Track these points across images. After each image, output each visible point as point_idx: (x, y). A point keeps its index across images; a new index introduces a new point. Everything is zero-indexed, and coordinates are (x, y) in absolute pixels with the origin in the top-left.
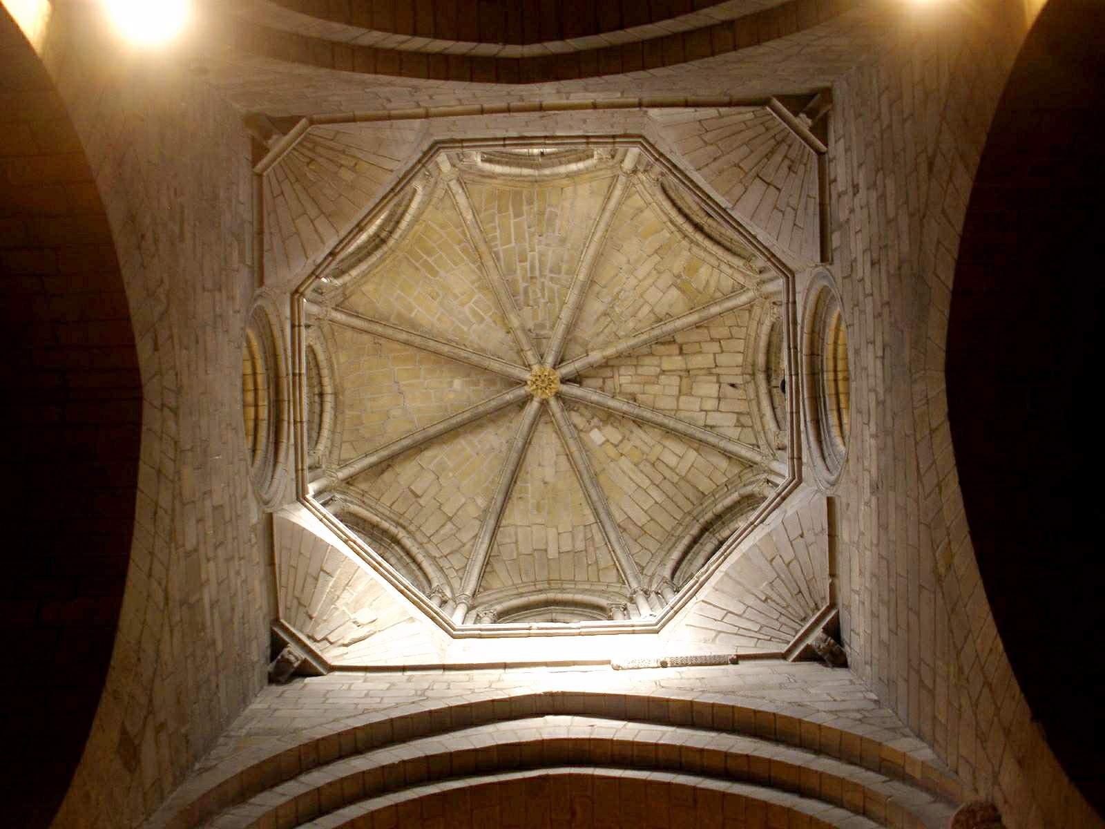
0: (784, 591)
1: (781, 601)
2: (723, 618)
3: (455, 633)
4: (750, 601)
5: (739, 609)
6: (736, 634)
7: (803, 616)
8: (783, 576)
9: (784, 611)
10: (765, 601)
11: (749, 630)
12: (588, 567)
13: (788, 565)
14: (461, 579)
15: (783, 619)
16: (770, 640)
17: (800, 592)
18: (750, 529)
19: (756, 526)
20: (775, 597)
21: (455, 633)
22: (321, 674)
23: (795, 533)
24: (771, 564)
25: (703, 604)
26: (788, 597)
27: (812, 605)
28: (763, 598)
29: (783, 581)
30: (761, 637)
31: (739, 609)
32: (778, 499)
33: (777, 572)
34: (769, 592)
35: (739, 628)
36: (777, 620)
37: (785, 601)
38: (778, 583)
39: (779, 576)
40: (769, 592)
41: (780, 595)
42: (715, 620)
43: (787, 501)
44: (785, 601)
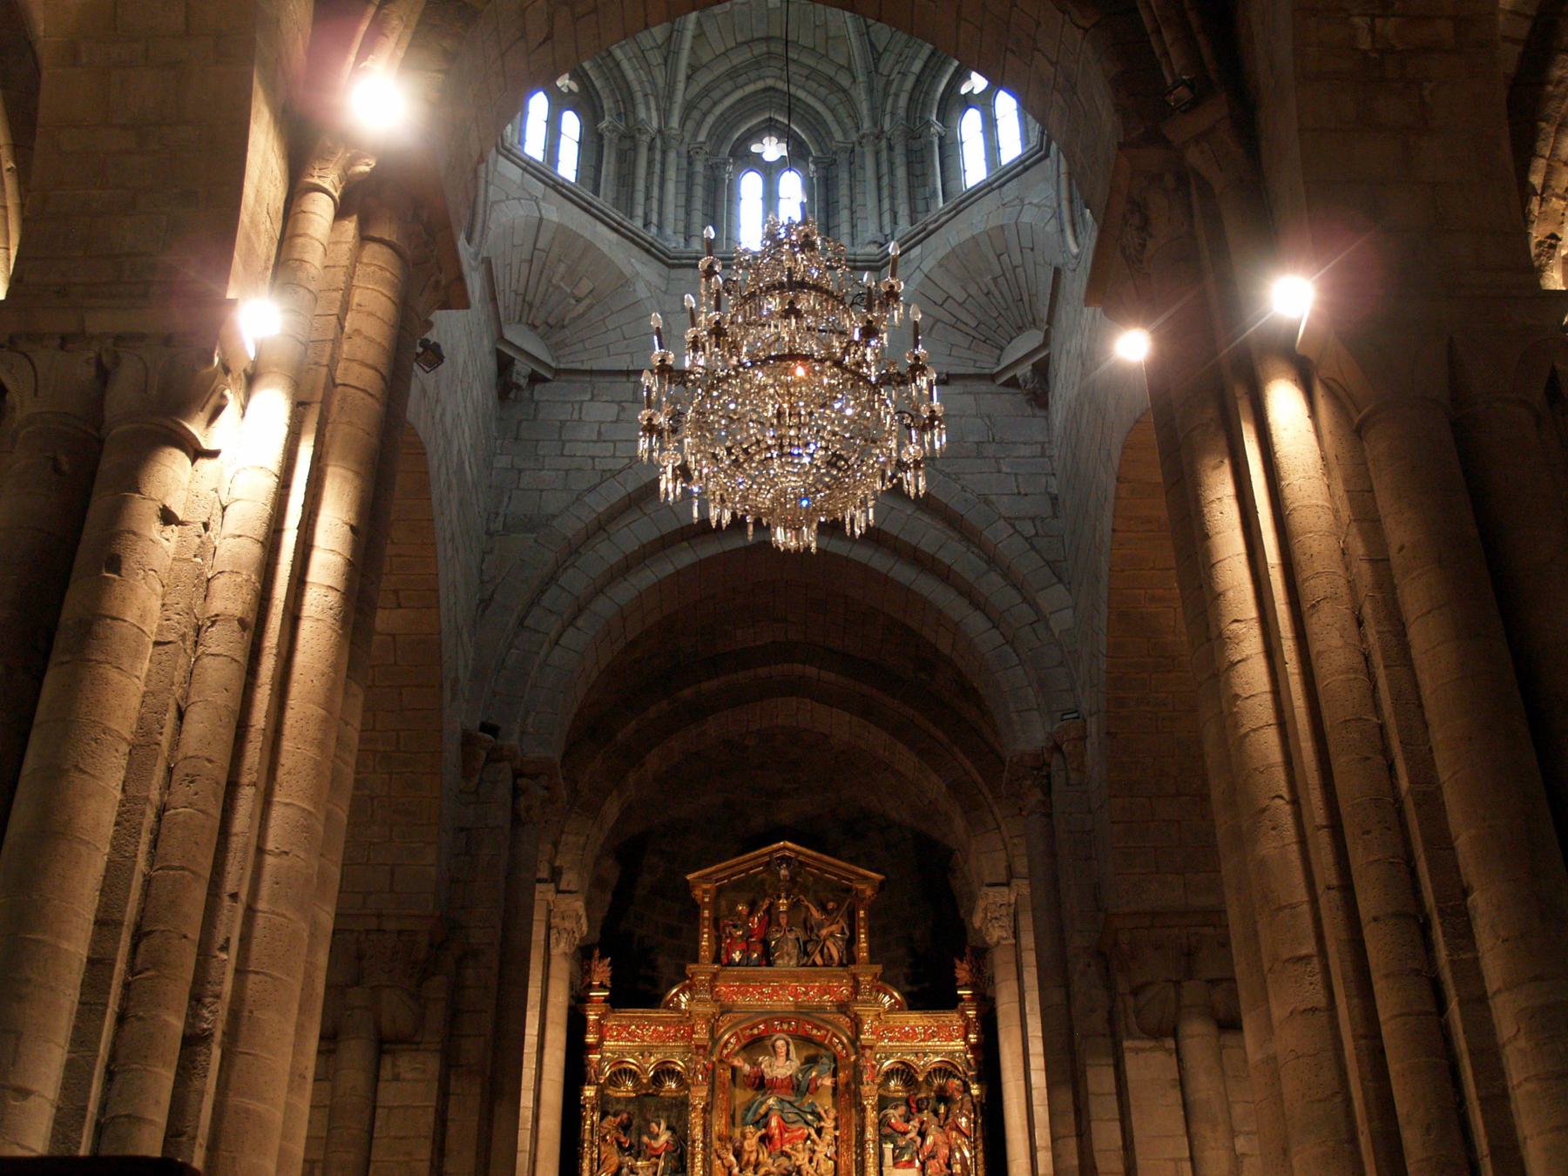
0: (1005, 289)
1: (1002, 302)
2: (944, 302)
3: (670, 261)
4: (973, 289)
5: (960, 295)
6: (953, 327)
7: (1021, 325)
8: (1008, 276)
9: (1003, 312)
10: (988, 293)
11: (966, 324)
12: (815, 29)
13: (1015, 268)
14: (666, 65)
15: (1001, 320)
16: (985, 342)
17: (1021, 300)
18: (986, 190)
19: (993, 190)
20: (996, 293)
21: (670, 261)
22: (545, 380)
23: (1027, 243)
24: (999, 259)
25: (926, 279)
26: (1010, 300)
27: (1030, 318)
28: (985, 291)
29: (1007, 280)
30: (977, 335)
31: (960, 295)
32: (1021, 167)
33: (1002, 268)
34: (993, 288)
35: (958, 319)
36: (995, 319)
37: (1006, 302)
38: (1001, 280)
39: (1004, 275)
40: (993, 288)
41: (1001, 293)
42: (935, 303)
43: (1028, 172)
44: (1006, 302)
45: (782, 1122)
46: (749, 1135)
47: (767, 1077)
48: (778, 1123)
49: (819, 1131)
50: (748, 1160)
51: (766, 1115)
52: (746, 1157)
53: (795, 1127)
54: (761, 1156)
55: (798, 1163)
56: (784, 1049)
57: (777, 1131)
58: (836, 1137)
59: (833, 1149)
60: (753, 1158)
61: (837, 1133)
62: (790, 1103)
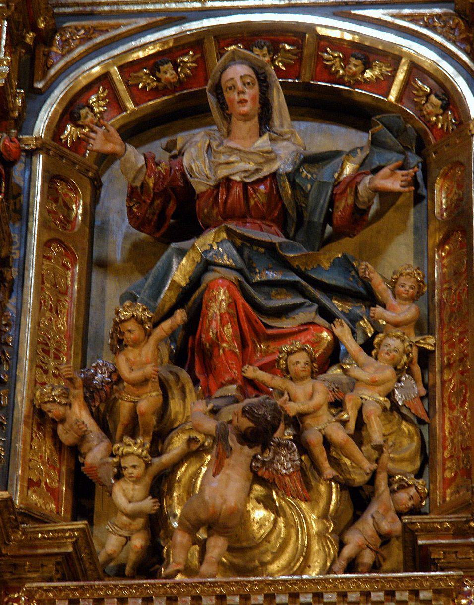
45: (242, 301)
46: (133, 331)
47: (200, 186)
48: (233, 304)
49: (368, 346)
50: (134, 417)
51: (195, 282)
52: (125, 408)
53: (287, 324)
54: (175, 405)
55: (292, 408)
56: (252, 93)
57: (228, 330)
58: (425, 357)
59: (418, 389)
60: (148, 402)
61: (429, 343)
62: (270, 248)
